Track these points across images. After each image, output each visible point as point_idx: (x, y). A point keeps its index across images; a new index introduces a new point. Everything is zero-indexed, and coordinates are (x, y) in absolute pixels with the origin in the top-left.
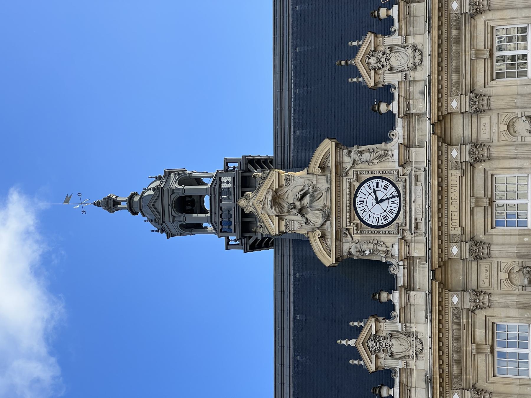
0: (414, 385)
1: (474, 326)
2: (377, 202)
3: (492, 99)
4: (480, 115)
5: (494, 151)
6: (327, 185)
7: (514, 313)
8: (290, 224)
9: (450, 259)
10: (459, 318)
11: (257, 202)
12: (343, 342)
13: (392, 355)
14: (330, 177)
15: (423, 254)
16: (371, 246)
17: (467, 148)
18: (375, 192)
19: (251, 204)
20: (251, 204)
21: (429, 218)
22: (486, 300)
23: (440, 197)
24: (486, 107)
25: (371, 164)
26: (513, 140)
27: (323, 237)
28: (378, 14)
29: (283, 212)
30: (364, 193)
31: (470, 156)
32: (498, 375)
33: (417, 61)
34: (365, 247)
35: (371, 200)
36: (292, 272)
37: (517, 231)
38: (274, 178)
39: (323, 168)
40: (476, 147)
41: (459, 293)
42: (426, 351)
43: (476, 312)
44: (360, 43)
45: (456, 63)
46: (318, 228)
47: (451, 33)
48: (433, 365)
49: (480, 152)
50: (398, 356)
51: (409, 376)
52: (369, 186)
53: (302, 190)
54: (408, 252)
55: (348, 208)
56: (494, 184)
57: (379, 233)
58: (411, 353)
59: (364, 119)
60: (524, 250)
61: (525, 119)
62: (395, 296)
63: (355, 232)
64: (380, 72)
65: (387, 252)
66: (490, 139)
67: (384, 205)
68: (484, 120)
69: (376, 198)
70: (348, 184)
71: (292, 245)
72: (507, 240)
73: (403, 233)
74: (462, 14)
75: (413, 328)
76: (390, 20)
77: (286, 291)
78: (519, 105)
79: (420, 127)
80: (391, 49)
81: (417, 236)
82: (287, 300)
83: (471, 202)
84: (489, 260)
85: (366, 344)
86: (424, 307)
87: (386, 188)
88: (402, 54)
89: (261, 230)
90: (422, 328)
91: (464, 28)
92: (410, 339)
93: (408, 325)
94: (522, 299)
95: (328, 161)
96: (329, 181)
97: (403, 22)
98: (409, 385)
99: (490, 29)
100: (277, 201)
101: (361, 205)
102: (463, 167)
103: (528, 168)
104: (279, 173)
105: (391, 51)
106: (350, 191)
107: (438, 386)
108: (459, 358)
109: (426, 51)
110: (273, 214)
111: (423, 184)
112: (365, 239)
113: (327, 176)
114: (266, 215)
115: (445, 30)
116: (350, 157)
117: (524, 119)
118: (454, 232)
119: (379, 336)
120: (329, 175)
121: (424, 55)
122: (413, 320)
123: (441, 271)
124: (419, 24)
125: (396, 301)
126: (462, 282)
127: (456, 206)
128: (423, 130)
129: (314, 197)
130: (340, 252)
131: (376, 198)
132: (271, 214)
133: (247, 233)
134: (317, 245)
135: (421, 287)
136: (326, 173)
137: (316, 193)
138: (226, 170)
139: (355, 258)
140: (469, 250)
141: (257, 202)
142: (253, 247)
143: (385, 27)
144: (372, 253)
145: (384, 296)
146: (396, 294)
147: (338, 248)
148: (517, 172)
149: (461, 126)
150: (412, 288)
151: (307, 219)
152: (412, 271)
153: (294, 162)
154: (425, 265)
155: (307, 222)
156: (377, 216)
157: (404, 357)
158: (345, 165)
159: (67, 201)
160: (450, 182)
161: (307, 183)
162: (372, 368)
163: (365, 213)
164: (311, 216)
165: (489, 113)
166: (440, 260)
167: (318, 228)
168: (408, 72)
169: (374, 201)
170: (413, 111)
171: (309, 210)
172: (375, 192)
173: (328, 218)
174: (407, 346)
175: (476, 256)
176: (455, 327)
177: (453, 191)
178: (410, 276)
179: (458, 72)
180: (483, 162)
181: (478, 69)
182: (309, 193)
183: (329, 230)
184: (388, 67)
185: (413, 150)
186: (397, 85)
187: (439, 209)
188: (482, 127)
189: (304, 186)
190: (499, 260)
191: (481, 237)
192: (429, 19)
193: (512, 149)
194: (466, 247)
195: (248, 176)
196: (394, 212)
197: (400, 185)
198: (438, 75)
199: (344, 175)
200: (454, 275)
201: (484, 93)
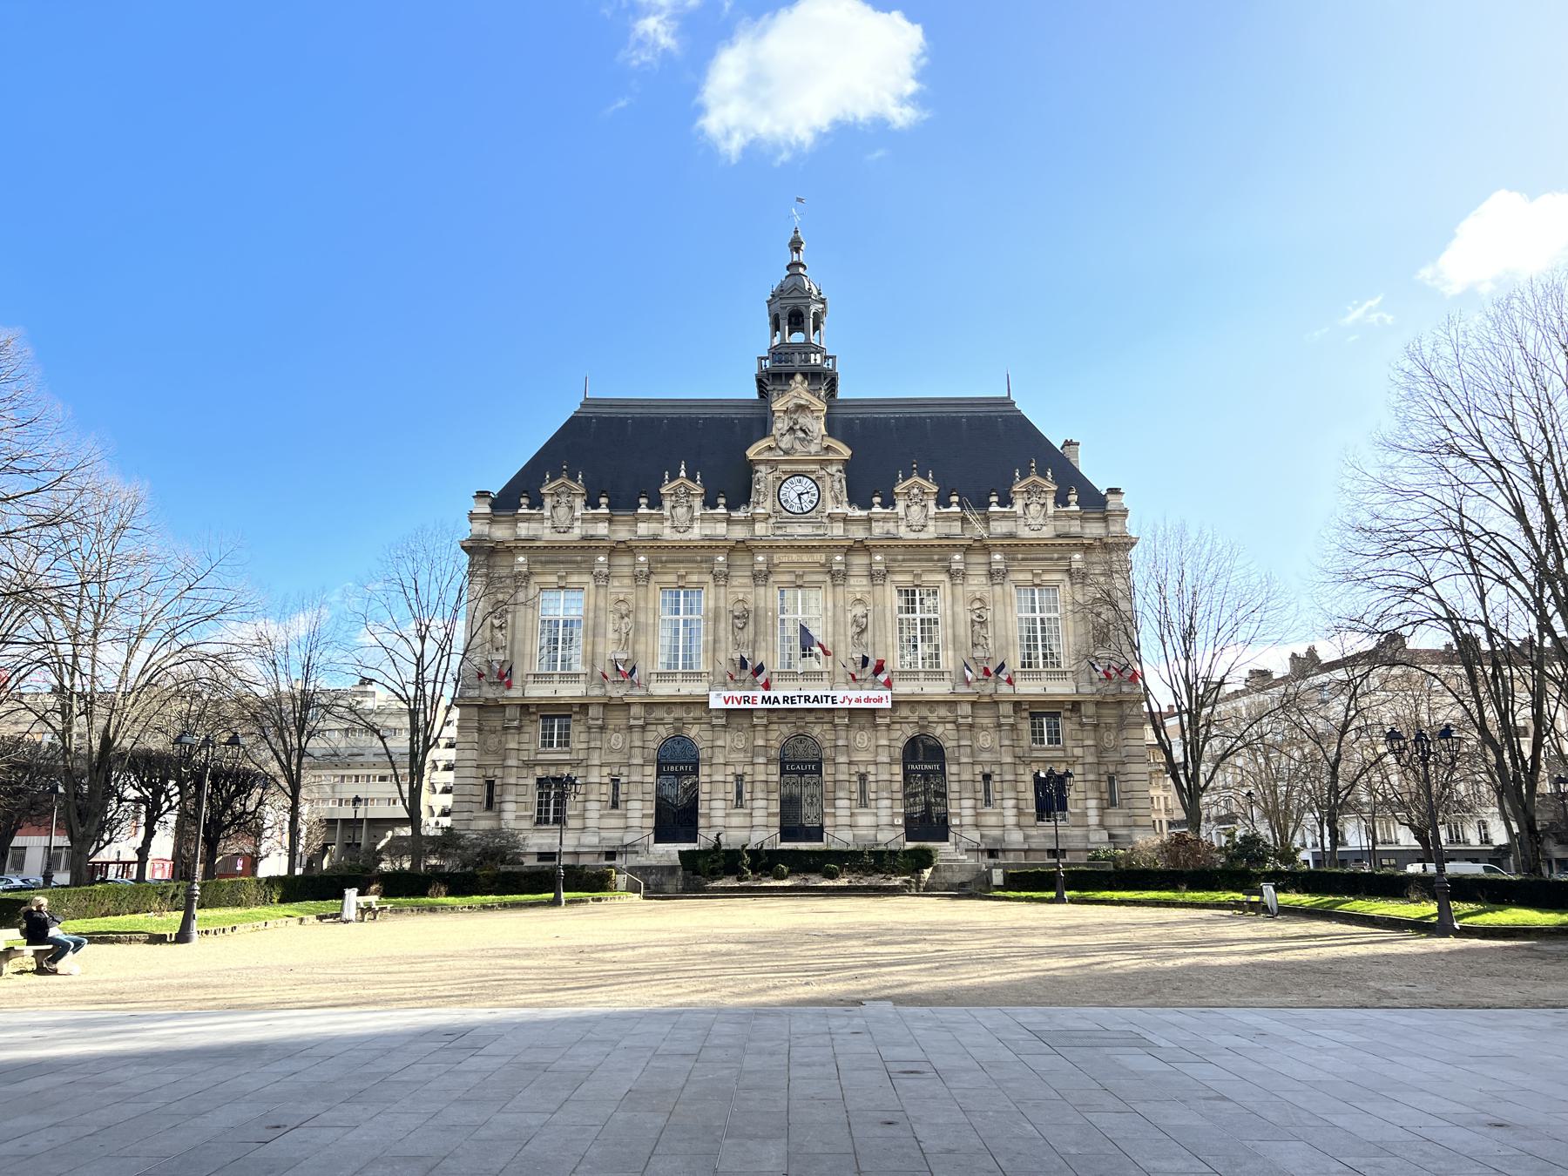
5: (839, 590)
7: (711, 604)
11: (799, 390)
15: (757, 533)
17: (842, 568)
27: (770, 448)
35: (800, 489)
39: (828, 448)
54: (759, 521)
59: (868, 484)
60: (761, 612)
62: (722, 510)
68: (865, 581)
72: (769, 600)
75: (697, 525)
76: (949, 505)
90: (697, 532)
94: (723, 612)
109: (922, 535)
128: (858, 533)
133: (773, 378)
134: (763, 444)
138: (827, 358)
141: (799, 390)
142: (759, 381)
143: (942, 501)
145: (722, 501)
147: (761, 462)
159: (799, 200)
162: (663, 491)
173: (786, 453)
197: (813, 514)
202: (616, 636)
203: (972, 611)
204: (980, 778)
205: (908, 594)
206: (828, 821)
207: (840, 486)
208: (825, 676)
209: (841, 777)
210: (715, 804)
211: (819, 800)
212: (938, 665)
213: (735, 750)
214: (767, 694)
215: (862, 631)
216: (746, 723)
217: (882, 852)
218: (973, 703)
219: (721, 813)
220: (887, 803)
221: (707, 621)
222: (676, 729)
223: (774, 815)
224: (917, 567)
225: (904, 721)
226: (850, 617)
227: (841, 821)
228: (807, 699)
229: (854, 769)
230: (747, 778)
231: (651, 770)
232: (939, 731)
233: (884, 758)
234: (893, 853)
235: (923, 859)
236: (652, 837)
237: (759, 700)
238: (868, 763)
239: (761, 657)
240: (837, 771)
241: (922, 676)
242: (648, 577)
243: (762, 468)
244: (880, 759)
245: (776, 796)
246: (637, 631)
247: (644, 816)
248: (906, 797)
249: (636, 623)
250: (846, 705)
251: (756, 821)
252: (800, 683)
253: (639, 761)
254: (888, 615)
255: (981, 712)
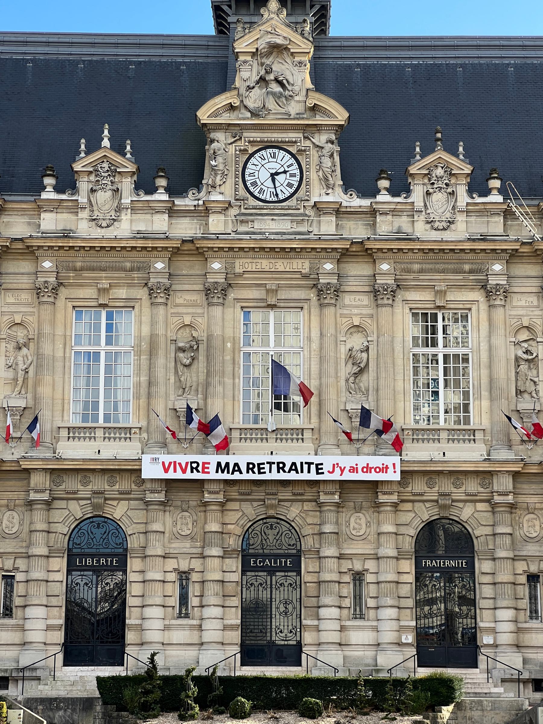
0: (60, 216)
1: (130, 286)
2: (272, 175)
3: (389, 309)
4: (372, 294)
5: (329, 312)
6: (293, 112)
7: (146, 330)
8: (247, 66)
9: (206, 260)
10: (139, 269)
12: (106, 132)
13: (93, 191)
14: (303, 118)
16: (221, 167)
18: (285, 172)
19: (272, 16)
20: (272, 16)
21: (253, 237)
22: (160, 300)
23: (279, 250)
24: (380, 302)
25: (318, 168)
26: (342, 332)
27: (231, 108)
28: (494, 178)
29: (262, 57)
30: (284, 159)
31: (325, 284)
32: (74, 312)
33: (436, 225)
34: (220, 159)
35: (274, 167)
36: (187, 60)
37: (238, 335)
38: (303, 46)
39: (315, 109)
40: (335, 291)
41: (167, 270)
42: (99, 231)
43: (146, 288)
44: (461, 157)
45: (431, 269)
46: (242, 101)
47: (466, 263)
48: (84, 239)
49: (330, 296)
50: (92, 199)
51: (69, 211)
52: (292, 165)
53: (288, 82)
54: (215, 211)
55: (266, 139)
56: (292, 310)
57: (236, 177)
58: (96, 213)
60: (217, 343)
61: (365, 345)
62: (162, 196)
63: (237, 148)
64: (426, 181)
65: (214, 187)
66: (345, 306)
67: (269, 183)
68: (365, 300)
69: (277, 174)
70: (294, 140)
71: (221, 60)
72: (229, 325)
73: (236, 206)
74: (487, 275)
75: (126, 217)
76: (486, 192)
77: (163, 51)
78: (380, 339)
79: (360, 227)
80: (452, 193)
81: (233, 222)
82: (152, 52)
83: (272, 284)
84: (205, 303)
85: (105, 161)
86: (150, 229)
87: (290, 185)
88: (445, 206)
89: (239, 29)
90: (126, 227)
91: (471, 278)
92: (113, 213)
93: (129, 210)
94: (162, 340)
95: (322, 115)
96: (298, 116)
97: (483, 207)
98: (59, 210)
99: (468, 306)
100: (275, 50)
101: (269, 155)
102: (312, 276)
103: (310, 348)
104: (308, 53)
105: (450, 193)
106: (286, 142)
107: (60, 245)
108: (93, 269)
110: (259, 45)
111: (293, 230)
112: (230, 160)
113: (304, 114)
114: (258, 36)
115: (471, 256)
116: (327, 143)
117: (366, 344)
118: (237, 265)
119: (114, 176)
120: (305, 116)
121: (443, 232)
122: (135, 217)
123: (193, 250)
124: (478, 226)
125: (156, 197)
126: (179, 272)
127: (268, 267)
128: (357, 231)
129: (279, 98)
130: (214, 129)
131: (277, 174)
132: (259, 42)
134: (221, 100)
135: (173, 225)
136: (308, 112)
137: (284, 99)
139: (207, 147)
140: (216, 283)
143: (477, 187)
144: (213, 168)
145: (162, 182)
146: (165, 197)
147: (218, 127)
148: (306, 335)
149: (359, 273)
150: (172, 214)
151: (253, 87)
152: (192, 215)
153: (322, 64)
154: (198, 232)
155: (250, 89)
156: (256, 174)
157: (91, 205)
158: (316, 135)
160: (295, 262)
161: (296, 88)
163: (260, 159)
164: (257, 92)
165: (373, 305)
166: (205, 249)
167: (242, 101)
168: (424, 213)
169: (273, 171)
170: (379, 219)
171: (264, 90)
172: (285, 172)
173: (254, 114)
174: (104, 209)
175: (209, 290)
176: (128, 265)
177: (285, 265)
178: (186, 213)
179: (421, 271)
180: (318, 298)
181: (424, 293)
182: (284, 90)
183: (240, 116)
184: (431, 191)
185: (334, 219)
186: (409, 200)
187: (264, 248)
188: (357, 297)
189: (293, 85)
190: (206, 315)
191: (232, 295)
192: (484, 239)
193: (332, 331)
194: (221, 279)
195: (305, 5)
196: (261, 195)
197: (293, 202)
198: (419, 249)
199: (306, 135)
200: (188, 264)
201: (396, 299)
202: (10, 374)
203: (517, 344)
204: (523, 579)
205: (428, 319)
206: (308, 637)
207: (332, 164)
208: (307, 435)
209: (326, 576)
210: (149, 612)
211: (296, 608)
212: (467, 421)
213: (177, 537)
214: (223, 459)
215: (361, 371)
216: (193, 499)
217: (383, 682)
218: (516, 475)
219: (159, 625)
220: (392, 613)
221: (139, 354)
222: (96, 507)
223: (231, 628)
224: (440, 281)
225: (418, 499)
226: (343, 350)
227: (326, 637)
228: (281, 467)
229: (346, 565)
230: (195, 577)
231: (60, 564)
232: (466, 513)
233: (389, 550)
234: (399, 684)
235: (440, 692)
236: (60, 657)
237: (213, 467)
238: (365, 557)
239: (215, 408)
240: (322, 569)
241: (444, 435)
242: (55, 290)
243: (219, 136)
244: (382, 552)
245: (236, 601)
246: (39, 367)
247: (49, 628)
248: (418, 604)
249: (39, 355)
250: (337, 476)
251: (207, 636)
252: (272, 444)
253: (43, 550)
254: (398, 348)
255: (526, 488)
